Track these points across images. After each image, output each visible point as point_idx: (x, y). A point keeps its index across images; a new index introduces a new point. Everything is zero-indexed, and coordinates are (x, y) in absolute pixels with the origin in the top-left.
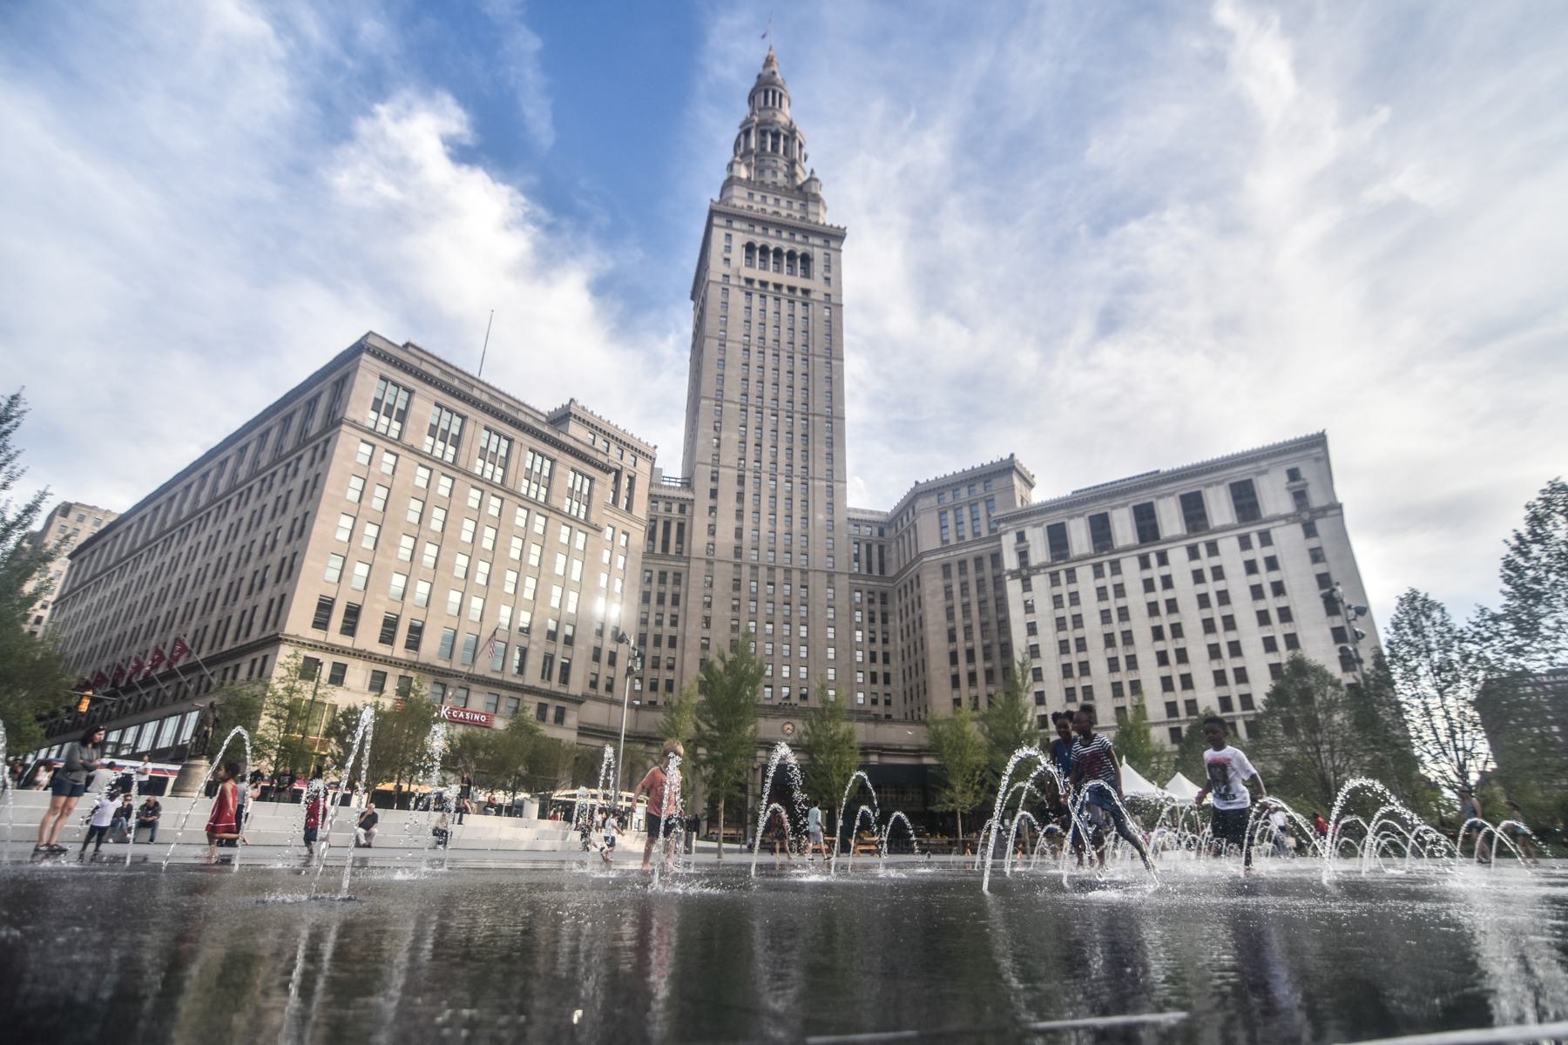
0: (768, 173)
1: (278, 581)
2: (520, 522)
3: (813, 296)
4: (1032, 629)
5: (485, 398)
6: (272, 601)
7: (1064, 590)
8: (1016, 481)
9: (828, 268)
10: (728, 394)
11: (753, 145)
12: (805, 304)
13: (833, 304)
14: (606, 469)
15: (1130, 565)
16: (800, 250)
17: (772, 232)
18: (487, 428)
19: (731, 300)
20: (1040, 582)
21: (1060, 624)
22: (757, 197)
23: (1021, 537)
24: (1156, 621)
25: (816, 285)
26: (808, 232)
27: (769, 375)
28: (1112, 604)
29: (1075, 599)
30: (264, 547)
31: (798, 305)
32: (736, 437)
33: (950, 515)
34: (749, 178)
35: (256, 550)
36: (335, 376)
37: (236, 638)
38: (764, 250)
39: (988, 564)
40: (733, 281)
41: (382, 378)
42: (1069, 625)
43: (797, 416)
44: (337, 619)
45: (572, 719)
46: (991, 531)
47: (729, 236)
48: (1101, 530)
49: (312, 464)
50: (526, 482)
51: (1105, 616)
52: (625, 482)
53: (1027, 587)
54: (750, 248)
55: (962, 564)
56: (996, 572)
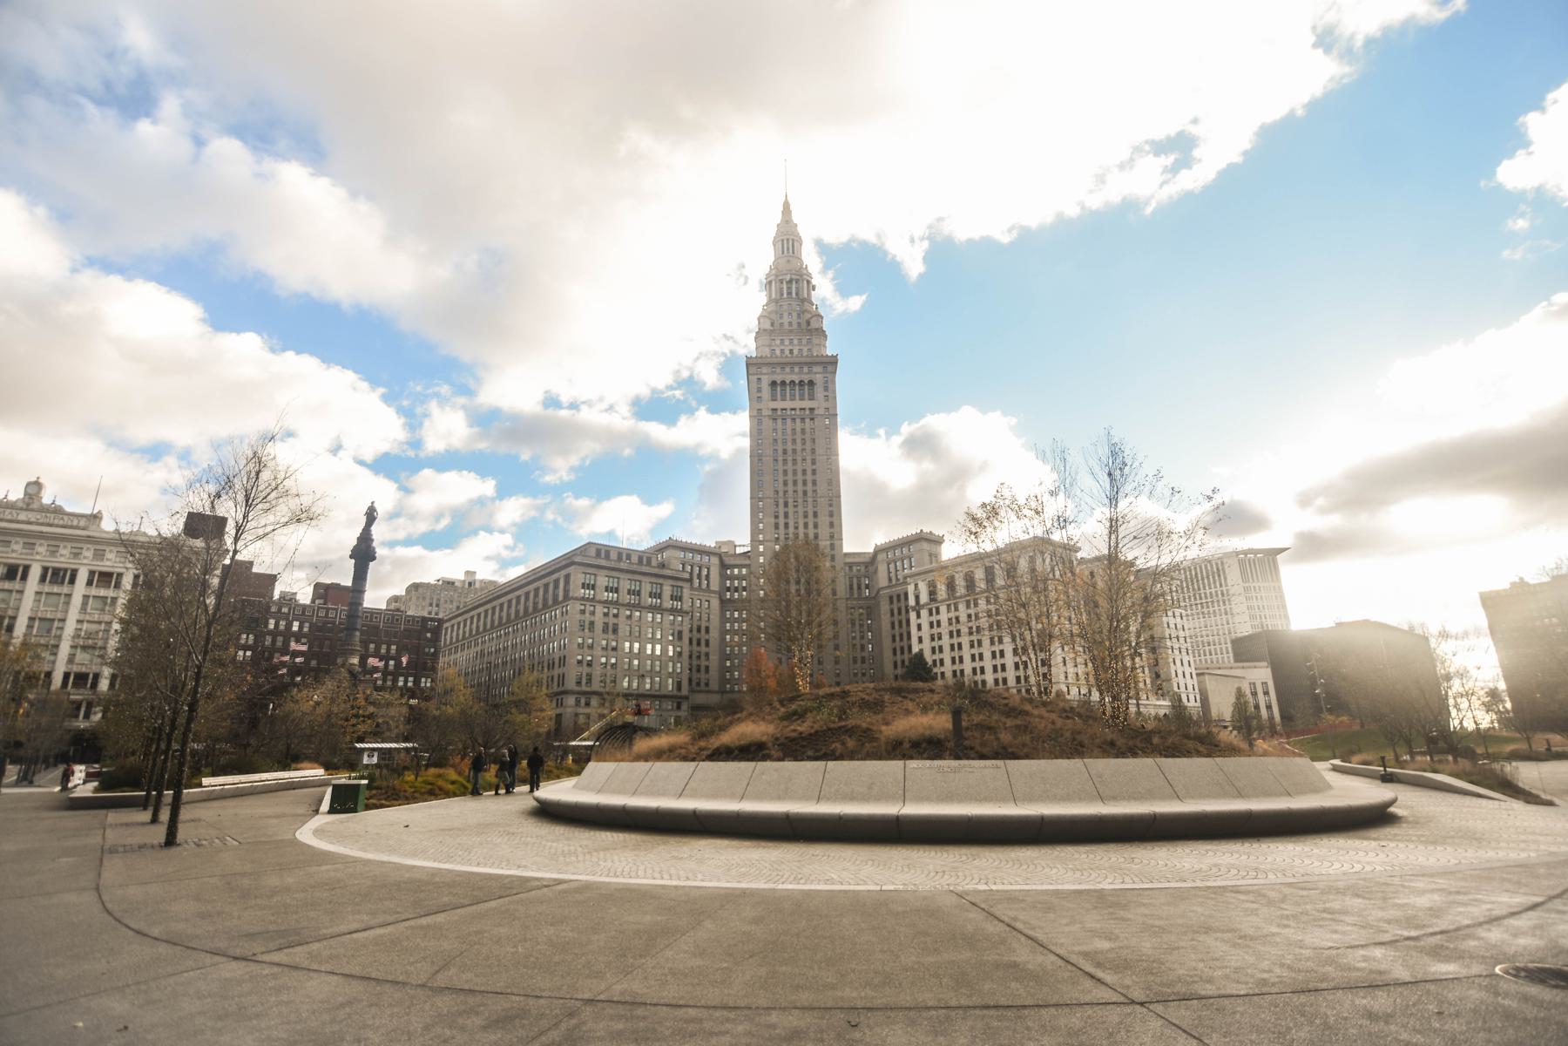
4: (920, 640)
7: (934, 618)
8: (925, 545)
9: (826, 389)
15: (962, 607)
16: (806, 378)
17: (788, 369)
20: (924, 613)
25: (819, 404)
26: (810, 364)
32: (773, 520)
38: (783, 383)
45: (685, 706)
48: (951, 586)
52: (705, 572)
54: (774, 383)
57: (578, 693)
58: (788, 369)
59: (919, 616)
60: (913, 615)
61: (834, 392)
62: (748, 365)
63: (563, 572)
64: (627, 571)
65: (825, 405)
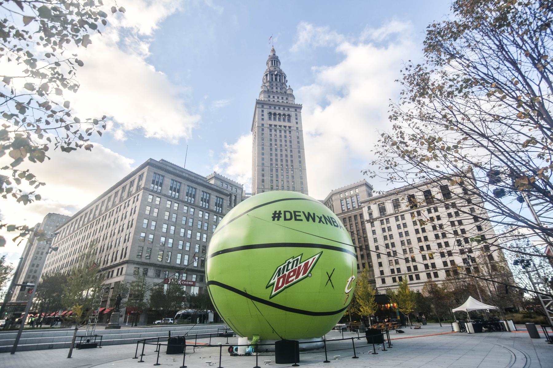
0: (274, 88)
1: (125, 242)
2: (201, 216)
3: (292, 128)
4: (375, 240)
5: (187, 176)
6: (123, 249)
9: (297, 119)
10: (266, 164)
11: (268, 79)
12: (290, 132)
13: (299, 130)
14: (227, 195)
17: (277, 108)
18: (188, 186)
19: (265, 132)
20: (377, 223)
21: (385, 238)
22: (272, 97)
23: (369, 208)
24: (419, 236)
26: (289, 107)
27: (279, 158)
28: (403, 230)
29: (389, 229)
30: (119, 231)
31: (288, 132)
32: (270, 178)
33: (344, 201)
34: (268, 90)
35: (116, 231)
36: (140, 173)
37: (112, 261)
38: (275, 114)
39: (359, 217)
40: (265, 126)
41: (155, 173)
42: (388, 238)
43: (290, 170)
44: (145, 254)
46: (359, 206)
47: (263, 111)
48: (396, 205)
49: (134, 203)
50: (201, 202)
51: (401, 235)
52: (233, 198)
53: (373, 226)
54: (270, 113)
55: (350, 217)
56: (362, 220)
57: (138, 263)
58: (277, 108)
59: (373, 226)
60: (368, 226)
61: (301, 121)
62: (258, 103)
63: (140, 173)
64: (188, 179)
65: (297, 126)
